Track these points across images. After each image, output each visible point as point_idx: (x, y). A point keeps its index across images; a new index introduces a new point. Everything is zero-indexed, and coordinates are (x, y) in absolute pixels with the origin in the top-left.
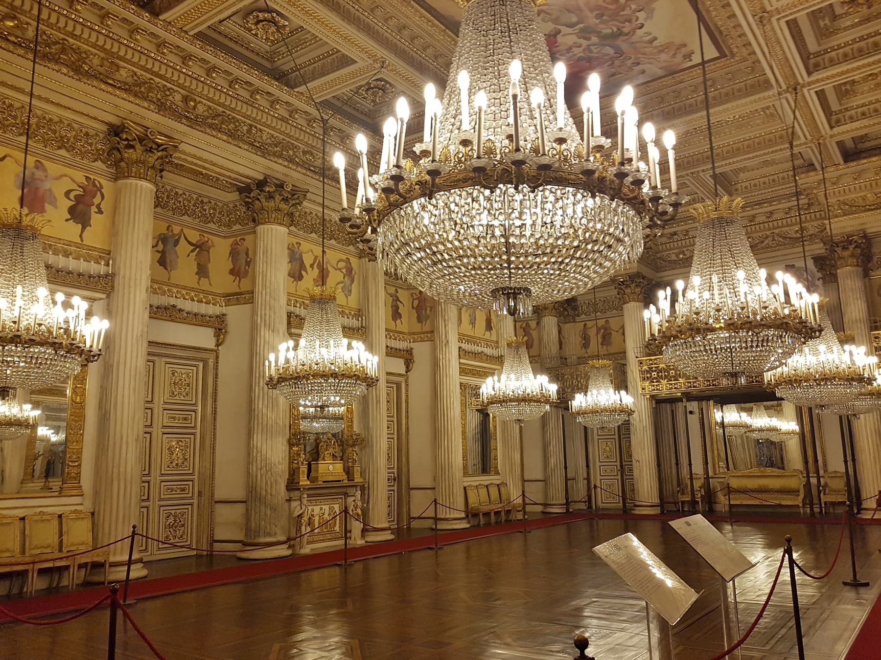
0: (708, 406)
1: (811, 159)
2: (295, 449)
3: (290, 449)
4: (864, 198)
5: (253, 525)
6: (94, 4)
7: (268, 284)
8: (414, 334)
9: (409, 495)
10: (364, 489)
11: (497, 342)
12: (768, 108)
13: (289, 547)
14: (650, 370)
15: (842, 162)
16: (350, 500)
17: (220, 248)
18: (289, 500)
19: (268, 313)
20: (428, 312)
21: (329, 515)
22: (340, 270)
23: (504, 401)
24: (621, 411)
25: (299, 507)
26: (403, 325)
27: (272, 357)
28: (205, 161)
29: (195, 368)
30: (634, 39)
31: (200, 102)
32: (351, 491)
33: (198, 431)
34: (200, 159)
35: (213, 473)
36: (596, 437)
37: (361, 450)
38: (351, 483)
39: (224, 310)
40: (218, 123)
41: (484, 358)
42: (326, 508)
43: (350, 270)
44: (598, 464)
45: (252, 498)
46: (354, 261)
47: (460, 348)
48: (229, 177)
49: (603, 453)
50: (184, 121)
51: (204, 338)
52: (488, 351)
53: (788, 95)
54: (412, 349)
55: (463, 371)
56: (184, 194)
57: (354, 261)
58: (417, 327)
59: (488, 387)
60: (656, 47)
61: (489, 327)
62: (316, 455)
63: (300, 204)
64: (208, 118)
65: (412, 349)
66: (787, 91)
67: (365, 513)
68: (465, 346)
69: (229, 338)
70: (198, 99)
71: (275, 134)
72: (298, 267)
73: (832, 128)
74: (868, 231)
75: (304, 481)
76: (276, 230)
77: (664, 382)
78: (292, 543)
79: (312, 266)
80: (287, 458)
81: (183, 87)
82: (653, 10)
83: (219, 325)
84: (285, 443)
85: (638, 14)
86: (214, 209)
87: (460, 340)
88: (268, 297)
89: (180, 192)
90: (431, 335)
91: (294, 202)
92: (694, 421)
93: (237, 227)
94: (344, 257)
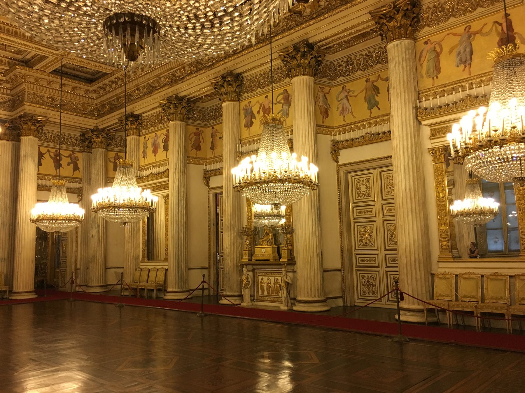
22: (279, 102)
38: (277, 262)
42: (272, 279)
79: (259, 112)
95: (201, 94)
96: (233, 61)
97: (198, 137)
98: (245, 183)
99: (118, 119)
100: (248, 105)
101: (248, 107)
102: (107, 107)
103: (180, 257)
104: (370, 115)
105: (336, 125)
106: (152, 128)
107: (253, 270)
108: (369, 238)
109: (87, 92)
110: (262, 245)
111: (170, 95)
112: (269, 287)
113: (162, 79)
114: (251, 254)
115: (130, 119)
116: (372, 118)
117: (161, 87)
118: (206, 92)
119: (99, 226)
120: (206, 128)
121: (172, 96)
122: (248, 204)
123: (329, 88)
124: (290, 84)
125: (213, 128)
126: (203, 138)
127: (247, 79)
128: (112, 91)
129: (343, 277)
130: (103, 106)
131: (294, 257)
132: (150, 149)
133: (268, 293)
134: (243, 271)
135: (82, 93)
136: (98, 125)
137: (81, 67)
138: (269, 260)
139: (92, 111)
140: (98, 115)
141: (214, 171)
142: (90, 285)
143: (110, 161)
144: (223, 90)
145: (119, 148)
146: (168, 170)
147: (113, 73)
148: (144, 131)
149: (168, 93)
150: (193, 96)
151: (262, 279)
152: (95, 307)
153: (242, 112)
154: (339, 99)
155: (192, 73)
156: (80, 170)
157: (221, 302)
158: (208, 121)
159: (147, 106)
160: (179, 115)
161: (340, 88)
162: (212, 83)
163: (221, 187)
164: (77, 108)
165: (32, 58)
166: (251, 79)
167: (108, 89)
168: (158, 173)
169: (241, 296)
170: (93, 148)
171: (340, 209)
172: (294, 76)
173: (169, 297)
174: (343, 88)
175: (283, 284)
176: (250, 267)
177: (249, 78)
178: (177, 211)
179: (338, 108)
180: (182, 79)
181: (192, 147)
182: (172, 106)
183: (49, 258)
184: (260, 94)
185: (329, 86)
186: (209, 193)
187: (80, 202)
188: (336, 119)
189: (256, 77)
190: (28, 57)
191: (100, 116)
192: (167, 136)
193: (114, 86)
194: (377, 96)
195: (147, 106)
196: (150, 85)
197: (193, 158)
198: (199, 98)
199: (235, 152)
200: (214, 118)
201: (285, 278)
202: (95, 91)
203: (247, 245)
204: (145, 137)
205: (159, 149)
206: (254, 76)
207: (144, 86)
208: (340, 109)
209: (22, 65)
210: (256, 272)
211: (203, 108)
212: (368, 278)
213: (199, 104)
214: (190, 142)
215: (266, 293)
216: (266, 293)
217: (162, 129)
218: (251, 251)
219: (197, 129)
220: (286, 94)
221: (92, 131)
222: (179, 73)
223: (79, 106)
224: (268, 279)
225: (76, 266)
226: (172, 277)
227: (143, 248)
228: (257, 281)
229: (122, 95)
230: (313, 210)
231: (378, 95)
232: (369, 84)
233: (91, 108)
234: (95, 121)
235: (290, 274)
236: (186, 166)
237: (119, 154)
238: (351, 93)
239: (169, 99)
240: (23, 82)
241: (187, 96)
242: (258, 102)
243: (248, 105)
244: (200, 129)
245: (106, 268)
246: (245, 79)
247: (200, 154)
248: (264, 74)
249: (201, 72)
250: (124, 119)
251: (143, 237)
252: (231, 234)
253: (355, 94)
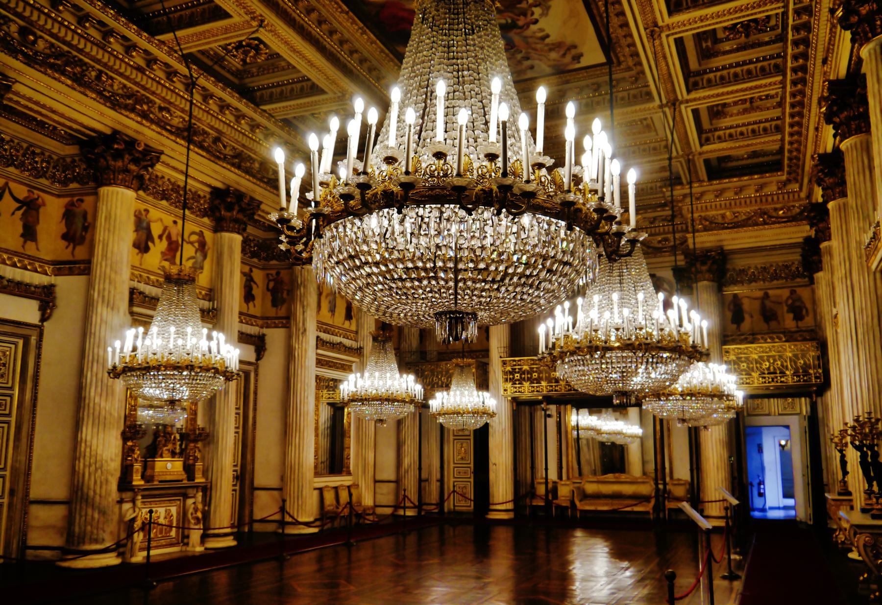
0: (565, 410)
1: (678, 173)
2: (130, 443)
3: (124, 443)
4: (723, 216)
5: (77, 529)
6: (75, 6)
7: (109, 255)
8: (268, 318)
9: (252, 494)
10: (207, 490)
11: (357, 332)
12: (645, 119)
13: (118, 556)
14: (513, 372)
15: (706, 179)
16: (190, 501)
17: (53, 209)
18: (121, 502)
19: (107, 286)
20: (285, 295)
21: (165, 518)
23: (366, 399)
24: (484, 413)
25: (131, 511)
26: (255, 309)
27: (117, 344)
28: (44, 106)
29: (13, 346)
30: (528, 33)
31: (41, 37)
32: (191, 492)
33: (13, 420)
34: (37, 103)
35: (30, 468)
36: (452, 438)
37: (204, 446)
38: (191, 483)
39: (53, 280)
40: (63, 64)
41: (343, 349)
43: (202, 246)
44: (452, 465)
45: (77, 497)
46: (208, 235)
47: (318, 337)
48: (70, 128)
49: (460, 455)
50: (20, 57)
51: (26, 311)
52: (347, 342)
53: (667, 110)
54: (264, 335)
55: (320, 363)
56: (12, 141)
57: (208, 235)
58: (272, 312)
59: (352, 384)
60: (547, 45)
61: (349, 316)
62: (152, 452)
63: (152, 166)
64: (49, 56)
65: (264, 335)
66: (666, 105)
67: (206, 516)
68: (323, 336)
69: (57, 314)
70: (39, 33)
71: (129, 84)
72: (144, 237)
73: (701, 145)
74: (726, 248)
75: (137, 481)
76: (123, 193)
77: (526, 384)
78: (121, 550)
79: (160, 237)
80: (120, 454)
81: (20, 16)
82: (548, 8)
83: (46, 299)
84: (119, 437)
85: (534, 9)
86: (48, 162)
87: (319, 329)
88: (108, 270)
89: (8, 138)
90: (287, 321)
91: (146, 163)
92: (552, 423)
93: (74, 186)
94: (197, 230)
96: (155, 134)
242: (161, 220)
243: (143, 213)
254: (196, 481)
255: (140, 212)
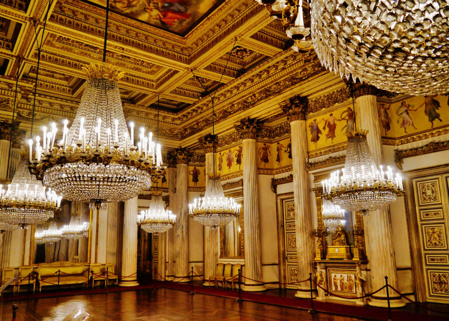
22: (344, 119)
38: (350, 261)
42: (345, 276)
79: (324, 128)
94: (346, 109)
95: (269, 115)
96: (299, 87)
97: (265, 151)
98: (337, 192)
99: (198, 139)
100: (314, 122)
101: (314, 124)
102: (189, 131)
103: (255, 255)
104: (432, 126)
105: (397, 136)
106: (226, 145)
107: (326, 268)
108: (438, 239)
109: (173, 119)
110: (335, 245)
111: (243, 117)
112: (342, 285)
113: (236, 105)
114: (324, 254)
115: (209, 139)
116: (435, 129)
117: (235, 112)
118: (274, 113)
119: (183, 227)
120: (272, 143)
121: (245, 119)
122: (318, 209)
123: (388, 105)
124: (354, 102)
125: (278, 143)
126: (270, 152)
127: (312, 101)
128: (193, 118)
129: (414, 276)
130: (186, 130)
131: (366, 257)
132: (225, 163)
133: (342, 289)
134: (316, 268)
135: (170, 120)
136: (181, 145)
137: (170, 100)
138: (343, 259)
139: (177, 134)
140: (181, 137)
141: (282, 180)
142: (177, 276)
143: (190, 174)
144: (291, 111)
145: (197, 163)
146: (242, 180)
147: (195, 104)
148: (219, 148)
149: (241, 117)
150: (262, 117)
151: (335, 276)
152: (182, 296)
153: (309, 129)
154: (399, 113)
155: (261, 99)
156: (167, 181)
157: (297, 295)
158: (274, 138)
159: (223, 128)
160: (251, 134)
161: (399, 104)
162: (281, 106)
163: (292, 193)
164: (166, 133)
165: (136, 97)
166: (315, 101)
167: (189, 116)
168: (234, 183)
169: (316, 291)
170: (178, 164)
171: (406, 212)
172: (359, 96)
173: (246, 289)
174: (402, 104)
175: (358, 282)
176: (323, 265)
177: (314, 100)
178: (252, 215)
179: (398, 122)
180: (253, 105)
181: (261, 159)
182: (245, 127)
183: (142, 252)
184: (325, 113)
185: (388, 103)
186: (277, 199)
187: (168, 208)
188: (397, 130)
189: (320, 98)
190: (133, 96)
191: (183, 137)
192: (240, 151)
193: (194, 114)
194: (438, 109)
195: (223, 128)
196: (225, 111)
197: (262, 169)
198: (267, 119)
199: (304, 163)
200: (280, 135)
201: (359, 275)
202: (179, 118)
203: (319, 245)
204: (220, 154)
205: (233, 163)
206: (319, 98)
207: (220, 112)
208: (401, 122)
209: (128, 103)
210: (329, 270)
211: (269, 127)
212: (440, 276)
213: (266, 124)
214: (259, 156)
215: (339, 289)
216: (339, 289)
217: (235, 146)
218: (323, 250)
219: (265, 145)
220: (350, 112)
221: (177, 150)
222: (250, 100)
223: (168, 131)
224: (341, 276)
225: (165, 260)
226: (248, 273)
227: (221, 246)
228: (330, 278)
229: (201, 120)
230: (385, 214)
231: (439, 108)
232: (429, 99)
233: (176, 132)
234: (179, 142)
235: (364, 272)
236: (257, 177)
237: (197, 168)
238: (410, 108)
239: (243, 121)
240: (128, 115)
241: (257, 117)
242: (323, 119)
243: (314, 122)
244: (267, 144)
245: (189, 262)
246: (310, 101)
247: (268, 166)
248: (328, 96)
249: (270, 97)
250: (203, 139)
251: (220, 237)
252: (303, 235)
253: (415, 108)
254: (353, 259)
255: (312, 123)
